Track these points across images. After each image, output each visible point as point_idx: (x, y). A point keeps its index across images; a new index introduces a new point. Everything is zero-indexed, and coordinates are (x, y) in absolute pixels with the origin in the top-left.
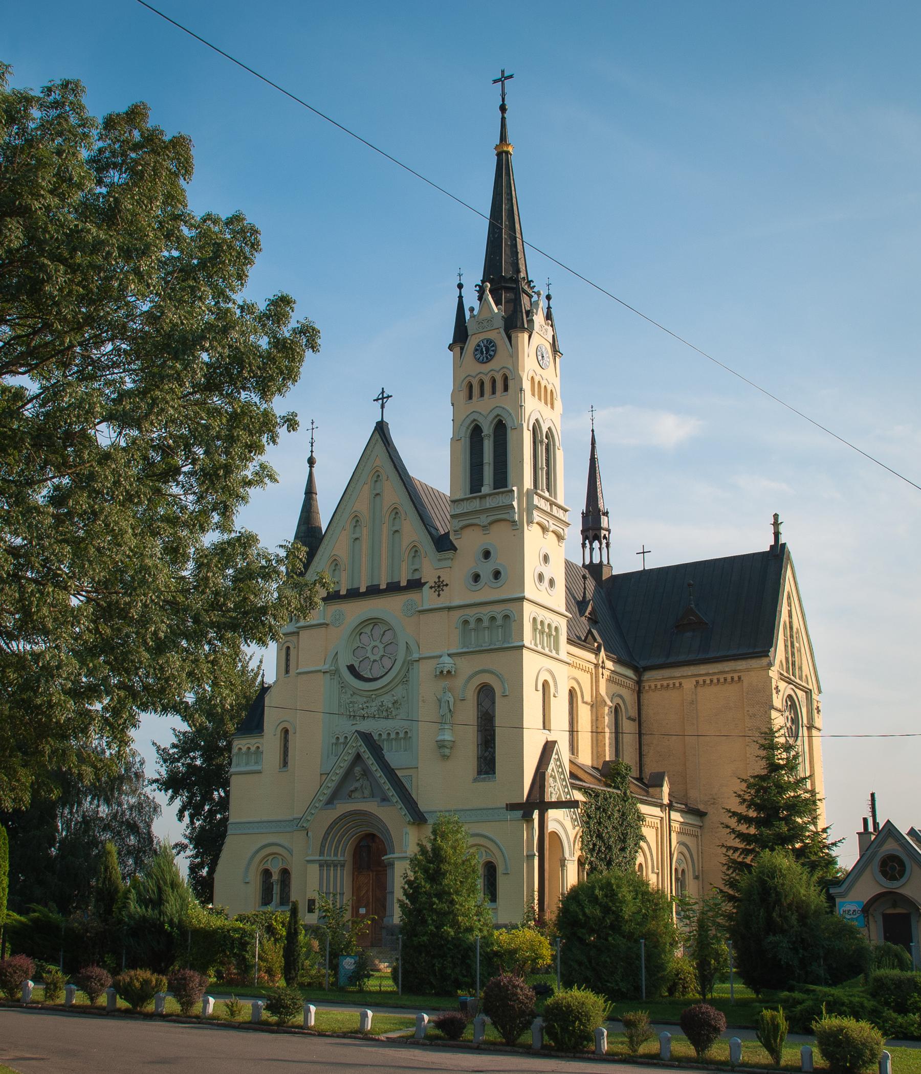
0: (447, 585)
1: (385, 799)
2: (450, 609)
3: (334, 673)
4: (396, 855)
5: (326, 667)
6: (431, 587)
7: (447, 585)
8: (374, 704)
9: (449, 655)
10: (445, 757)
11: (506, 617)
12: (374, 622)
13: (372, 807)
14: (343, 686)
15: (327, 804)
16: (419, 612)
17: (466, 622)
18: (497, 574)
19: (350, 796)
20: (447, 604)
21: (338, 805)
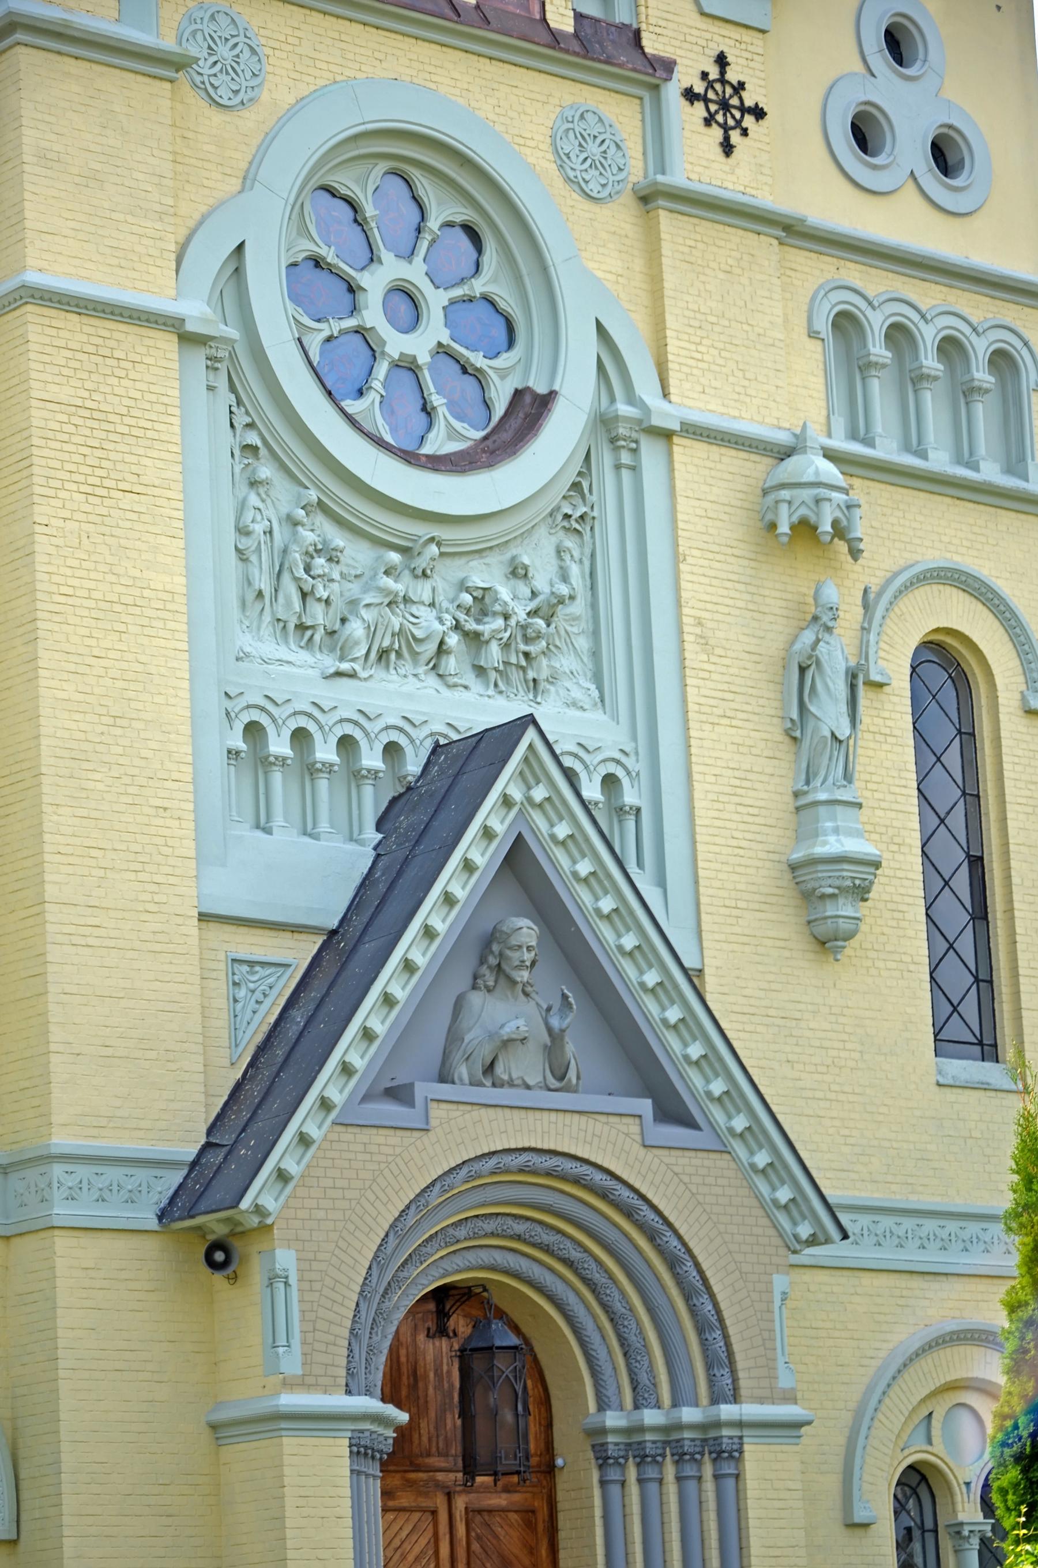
0: (759, 113)
1: (672, 1111)
2: (792, 231)
3: (225, 358)
4: (749, 1410)
5: (196, 310)
6: (690, 95)
7: (759, 113)
8: (423, 591)
9: (829, 455)
10: (827, 942)
11: (1002, 360)
12: (413, 157)
13: (610, 1137)
14: (263, 439)
15: (366, 1098)
16: (647, 198)
17: (846, 324)
18: (945, 154)
19: (490, 1069)
20: (767, 199)
21: (437, 1112)
